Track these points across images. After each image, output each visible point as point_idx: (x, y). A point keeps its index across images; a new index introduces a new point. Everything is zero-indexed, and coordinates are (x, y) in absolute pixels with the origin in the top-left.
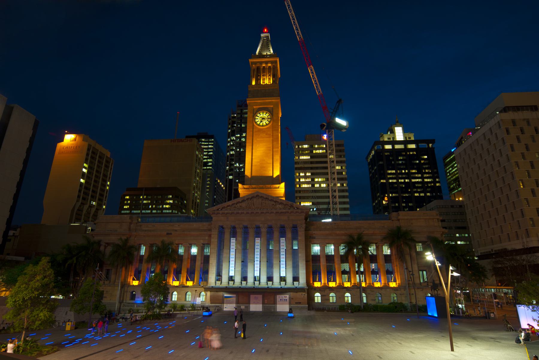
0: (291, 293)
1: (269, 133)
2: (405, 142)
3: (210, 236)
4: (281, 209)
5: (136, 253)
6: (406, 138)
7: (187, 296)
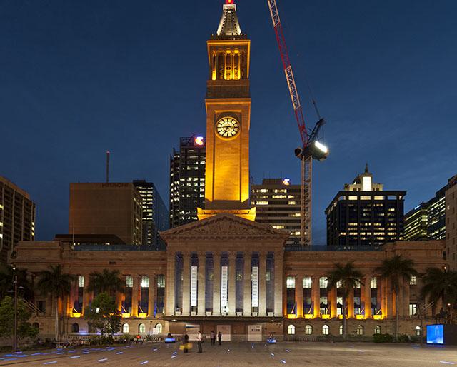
0: (265, 323)
1: (235, 147)
2: (373, 193)
3: (165, 266)
4: (254, 234)
5: (73, 283)
6: (374, 189)
7: (141, 329)
